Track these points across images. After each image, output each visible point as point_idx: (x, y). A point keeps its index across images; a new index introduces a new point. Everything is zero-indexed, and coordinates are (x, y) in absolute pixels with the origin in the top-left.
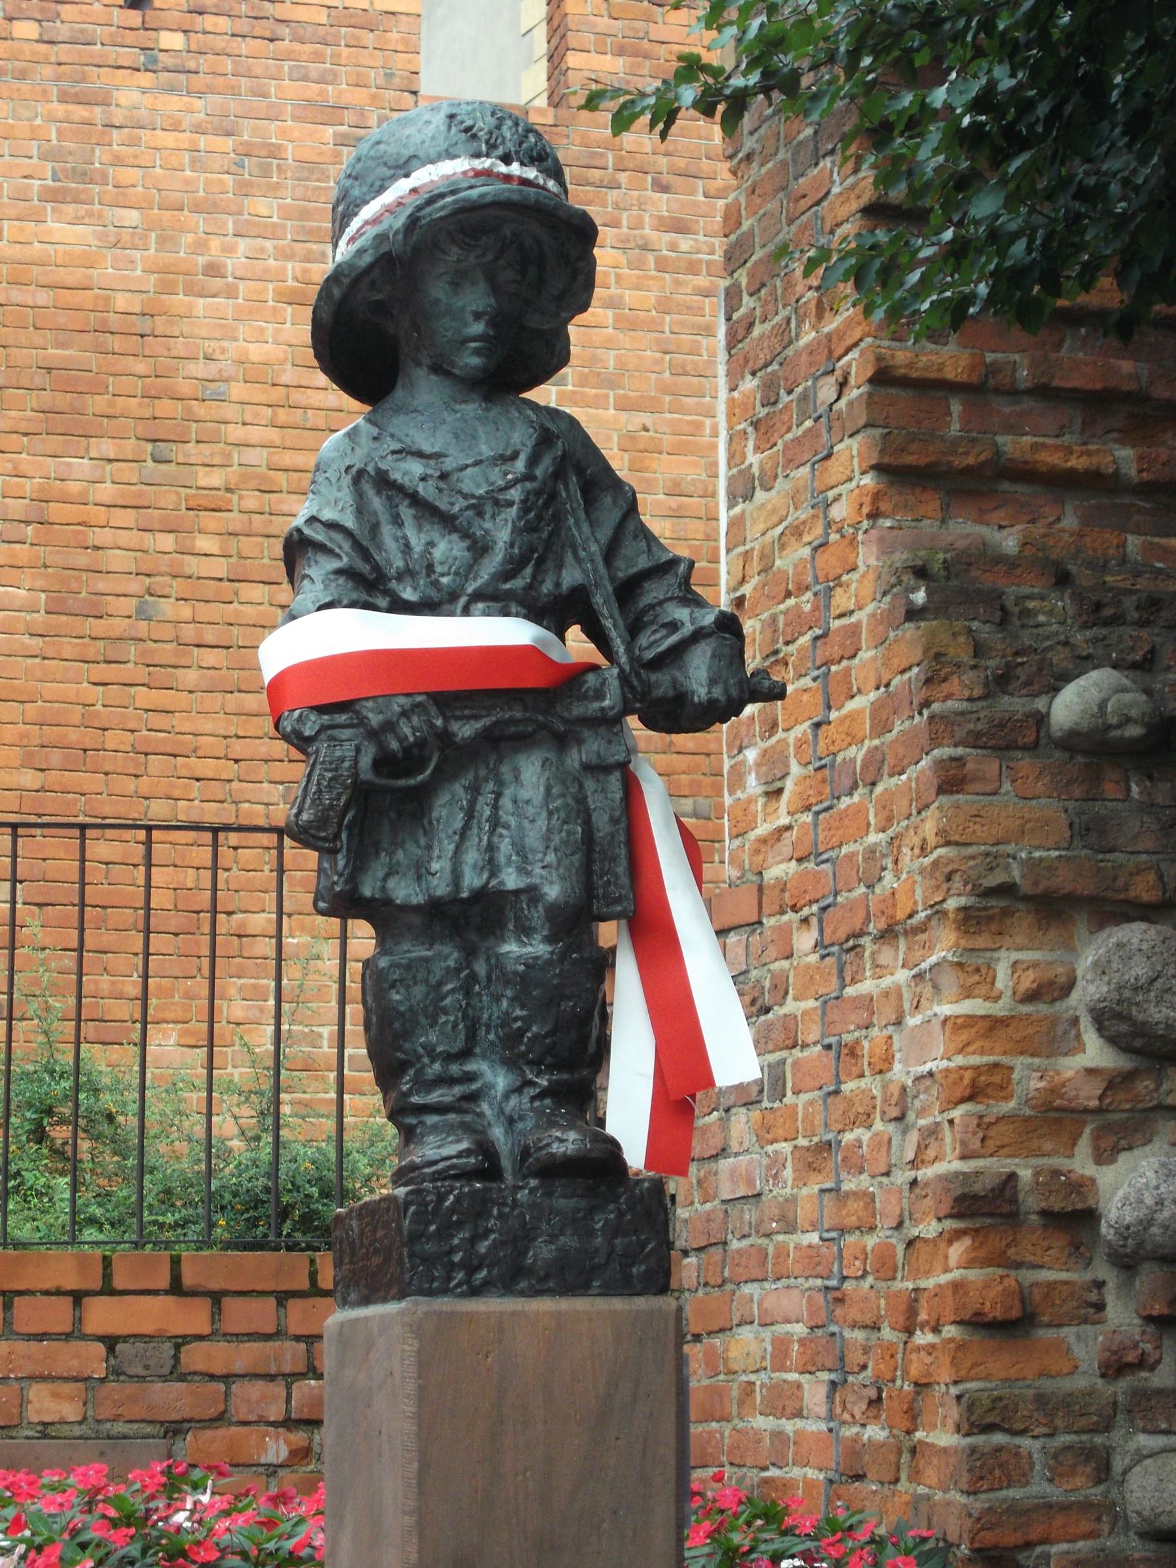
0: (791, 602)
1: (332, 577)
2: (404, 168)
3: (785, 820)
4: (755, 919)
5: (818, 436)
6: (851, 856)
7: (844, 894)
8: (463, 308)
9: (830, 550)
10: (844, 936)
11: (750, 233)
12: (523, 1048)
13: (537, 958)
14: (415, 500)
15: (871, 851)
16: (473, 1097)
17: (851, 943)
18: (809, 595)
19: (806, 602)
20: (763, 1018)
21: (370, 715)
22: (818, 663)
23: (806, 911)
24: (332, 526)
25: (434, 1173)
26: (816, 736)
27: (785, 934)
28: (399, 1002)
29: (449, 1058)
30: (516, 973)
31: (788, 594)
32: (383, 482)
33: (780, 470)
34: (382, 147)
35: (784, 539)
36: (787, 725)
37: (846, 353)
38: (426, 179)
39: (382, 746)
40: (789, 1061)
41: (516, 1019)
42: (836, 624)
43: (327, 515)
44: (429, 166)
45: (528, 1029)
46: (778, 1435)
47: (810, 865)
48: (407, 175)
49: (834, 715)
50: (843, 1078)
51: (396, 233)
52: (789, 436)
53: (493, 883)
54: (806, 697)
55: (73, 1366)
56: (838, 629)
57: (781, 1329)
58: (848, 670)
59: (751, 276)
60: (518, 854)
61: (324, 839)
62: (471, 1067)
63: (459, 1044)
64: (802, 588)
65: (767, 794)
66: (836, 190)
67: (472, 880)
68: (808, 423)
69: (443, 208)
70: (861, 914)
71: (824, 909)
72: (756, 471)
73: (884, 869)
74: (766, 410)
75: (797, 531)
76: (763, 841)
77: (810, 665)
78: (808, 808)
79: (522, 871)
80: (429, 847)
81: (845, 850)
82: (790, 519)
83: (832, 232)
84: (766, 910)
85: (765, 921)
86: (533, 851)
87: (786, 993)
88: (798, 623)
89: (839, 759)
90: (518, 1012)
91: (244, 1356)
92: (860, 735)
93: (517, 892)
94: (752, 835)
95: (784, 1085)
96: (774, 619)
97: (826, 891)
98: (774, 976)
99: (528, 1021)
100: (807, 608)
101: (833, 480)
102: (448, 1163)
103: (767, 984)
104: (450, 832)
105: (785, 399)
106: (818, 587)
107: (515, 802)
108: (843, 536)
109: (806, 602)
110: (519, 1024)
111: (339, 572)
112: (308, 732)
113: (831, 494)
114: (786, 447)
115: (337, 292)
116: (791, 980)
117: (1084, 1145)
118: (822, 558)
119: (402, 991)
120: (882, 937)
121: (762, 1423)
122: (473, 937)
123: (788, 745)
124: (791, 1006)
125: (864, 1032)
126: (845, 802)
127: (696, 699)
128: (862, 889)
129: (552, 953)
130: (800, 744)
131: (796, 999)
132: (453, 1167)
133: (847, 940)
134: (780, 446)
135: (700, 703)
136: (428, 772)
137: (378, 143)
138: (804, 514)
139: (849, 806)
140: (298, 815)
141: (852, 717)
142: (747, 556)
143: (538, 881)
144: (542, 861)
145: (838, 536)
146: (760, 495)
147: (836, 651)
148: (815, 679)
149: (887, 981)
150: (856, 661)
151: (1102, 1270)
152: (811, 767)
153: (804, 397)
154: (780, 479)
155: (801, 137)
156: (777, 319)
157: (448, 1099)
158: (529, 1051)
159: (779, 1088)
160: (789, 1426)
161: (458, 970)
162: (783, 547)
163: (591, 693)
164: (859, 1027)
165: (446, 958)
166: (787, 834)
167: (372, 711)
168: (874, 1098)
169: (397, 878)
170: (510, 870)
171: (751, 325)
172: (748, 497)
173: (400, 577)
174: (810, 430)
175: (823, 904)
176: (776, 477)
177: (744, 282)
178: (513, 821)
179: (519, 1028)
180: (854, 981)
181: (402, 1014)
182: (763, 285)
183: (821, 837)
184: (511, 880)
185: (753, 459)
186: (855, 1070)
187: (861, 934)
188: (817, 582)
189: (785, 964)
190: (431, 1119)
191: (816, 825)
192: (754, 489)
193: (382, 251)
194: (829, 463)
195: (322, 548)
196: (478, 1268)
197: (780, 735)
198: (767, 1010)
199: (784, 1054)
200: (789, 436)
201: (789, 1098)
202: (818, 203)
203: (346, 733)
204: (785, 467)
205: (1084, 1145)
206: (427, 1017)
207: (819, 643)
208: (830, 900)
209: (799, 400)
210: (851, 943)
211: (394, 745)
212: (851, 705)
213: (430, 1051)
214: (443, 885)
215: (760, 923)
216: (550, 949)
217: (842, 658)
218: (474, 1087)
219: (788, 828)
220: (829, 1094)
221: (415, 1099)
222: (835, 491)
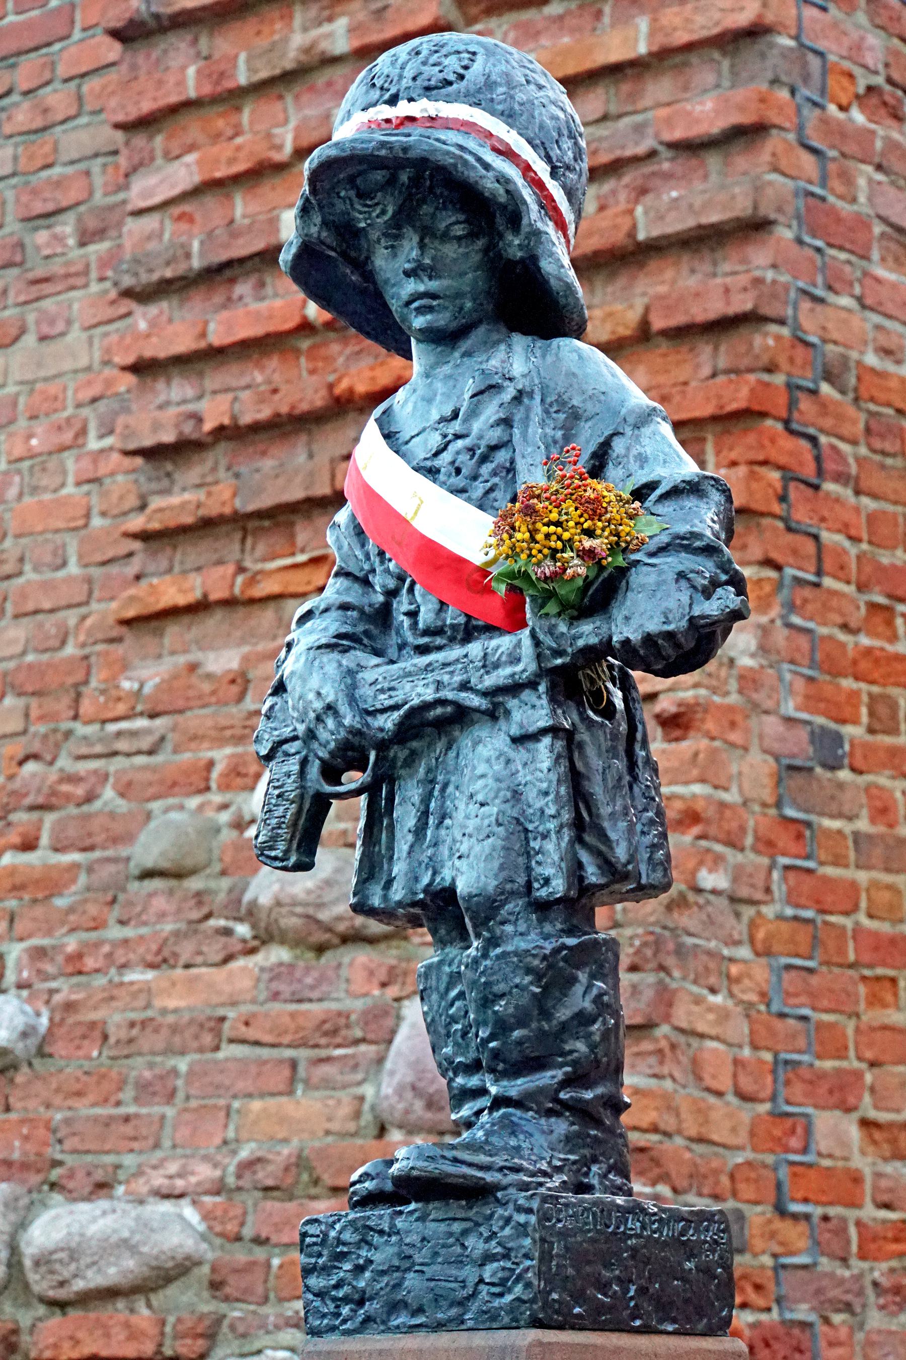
61: (275, 858)
196: (361, 1303)
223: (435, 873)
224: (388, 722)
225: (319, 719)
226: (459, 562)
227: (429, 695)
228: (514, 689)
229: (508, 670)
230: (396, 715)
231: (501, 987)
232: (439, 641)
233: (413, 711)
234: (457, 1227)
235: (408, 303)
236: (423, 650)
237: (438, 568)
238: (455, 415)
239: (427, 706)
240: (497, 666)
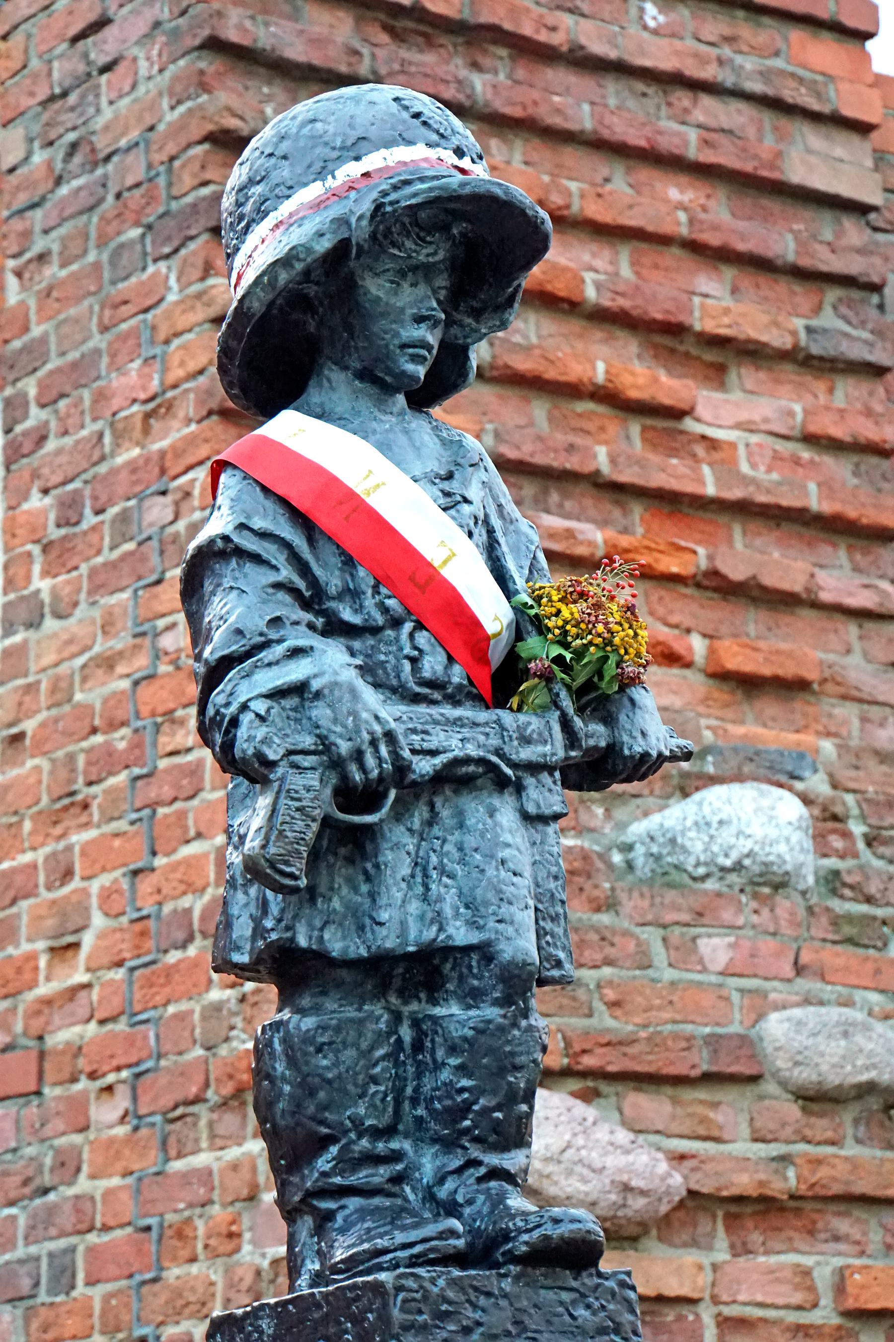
0: (98, 739)
1: (271, 591)
2: (355, 149)
3: (81, 977)
4: (33, 1087)
5: (144, 559)
6: (181, 1017)
7: (173, 1058)
8: (402, 310)
9: (157, 683)
10: (171, 1104)
11: (43, 340)
12: (467, 1123)
13: (489, 1022)
15: (217, 1007)
16: (398, 1179)
17: (179, 1111)
18: (125, 731)
19: (121, 740)
20: (38, 1201)
21: (339, 741)
22: (138, 804)
23: (111, 1078)
24: (264, 535)
25: (412, 1256)
26: (133, 885)
27: (79, 1105)
28: (327, 1068)
29: (378, 1133)
30: (465, 1039)
31: (94, 731)
33: (83, 596)
34: (319, 125)
35: (87, 671)
36: (88, 873)
37: (186, 472)
38: (381, 164)
39: (345, 777)
40: (81, 1249)
41: (462, 1090)
42: (163, 764)
43: (258, 523)
44: (383, 151)
45: (476, 1102)
47: (121, 1026)
48: (357, 158)
49: (160, 861)
50: (166, 1264)
51: (360, 218)
52: (100, 560)
53: (442, 937)
54: (117, 843)
56: (167, 771)
58: (182, 815)
59: (42, 386)
60: (467, 907)
62: (395, 1145)
63: (386, 1120)
64: (113, 725)
65: (52, 949)
66: (172, 297)
67: (419, 934)
68: (130, 546)
69: (415, 195)
70: (201, 1079)
71: (138, 1076)
72: (46, 596)
73: (232, 1028)
74: (63, 531)
75: (108, 663)
76: (48, 1002)
77: (126, 806)
78: (119, 964)
79: (473, 924)
80: (373, 896)
81: (171, 1009)
82: (97, 649)
83: (167, 342)
84: (49, 1076)
85: (46, 1091)
86: (487, 904)
87: (78, 1170)
88: (105, 763)
89: (167, 909)
90: (465, 1082)
92: (199, 883)
93: (468, 949)
94: (30, 996)
95: (74, 1276)
96: (71, 758)
97: (144, 1054)
98: (58, 1151)
99: (477, 1092)
100: (122, 745)
101: (162, 609)
102: (427, 1246)
103: (48, 1161)
104: (399, 877)
105: (90, 520)
106: (140, 723)
107: (461, 849)
108: (178, 668)
109: (121, 740)
110: (466, 1095)
111: (278, 586)
112: (272, 756)
113: (161, 623)
114: (93, 572)
115: (283, 277)
116: (85, 1156)
118: (146, 692)
119: (331, 1055)
120: (224, 1104)
122: (394, 1000)
123: (88, 895)
124: (83, 1185)
125: (198, 1211)
126: (174, 957)
127: (626, 752)
128: (199, 1052)
129: (504, 1016)
130: (106, 895)
131: (93, 1177)
132: (432, 1250)
133: (176, 1107)
134: (84, 569)
135: (632, 757)
136: (385, 810)
137: (314, 121)
138: (121, 642)
139: (180, 961)
140: (264, 847)
141: (189, 863)
143: (493, 937)
144: (494, 914)
145: (170, 668)
146: (50, 624)
147: (167, 792)
148: (132, 823)
149: (233, 1153)
150: (195, 802)
152: (124, 920)
153: (124, 517)
154: (83, 606)
155: (123, 238)
156: (84, 433)
157: (376, 1180)
158: (475, 1126)
159: (65, 1280)
161: (389, 1034)
162: (84, 679)
163: (535, 736)
164: (191, 1206)
165: (378, 1019)
166: (83, 994)
167: (341, 736)
168: (212, 1284)
169: (332, 927)
170: (458, 923)
171: (42, 439)
172: (33, 624)
173: (340, 597)
174: (131, 553)
175: (137, 1070)
176: (76, 604)
177: (32, 392)
178: (458, 869)
179: (464, 1101)
180: (180, 1156)
181: (329, 1082)
182: (63, 396)
183: (137, 996)
184: (461, 934)
185: (42, 585)
186: (185, 1253)
187: (198, 1100)
188: (138, 717)
189: (77, 1139)
190: (353, 1203)
191: (131, 983)
192: (42, 616)
193: (340, 237)
194: (159, 588)
195: (257, 559)
197: (76, 883)
198: (46, 1191)
199: (74, 1240)
200: (100, 560)
201: (81, 1289)
202: (146, 310)
203: (307, 761)
204: (90, 593)
206: (356, 1085)
207: (140, 783)
208: (150, 1064)
209: (113, 521)
210: (179, 1111)
211: (358, 777)
212: (186, 851)
213: (358, 1123)
214: (393, 936)
215: (38, 1093)
216: (502, 1012)
217: (175, 799)
218: (399, 1167)
219: (87, 986)
220: (144, 1283)
221: (338, 1180)
222: (168, 620)
223: (441, 929)
225: (374, 743)
226: (476, 624)
227: (472, 751)
228: (534, 768)
229: (540, 749)
230: (438, 761)
231: (523, 1059)
232: (437, 696)
233: (457, 762)
234: (565, 1296)
235: (404, 346)
236: (416, 699)
237: (457, 624)
238: (450, 476)
239: (467, 760)
240: (526, 740)
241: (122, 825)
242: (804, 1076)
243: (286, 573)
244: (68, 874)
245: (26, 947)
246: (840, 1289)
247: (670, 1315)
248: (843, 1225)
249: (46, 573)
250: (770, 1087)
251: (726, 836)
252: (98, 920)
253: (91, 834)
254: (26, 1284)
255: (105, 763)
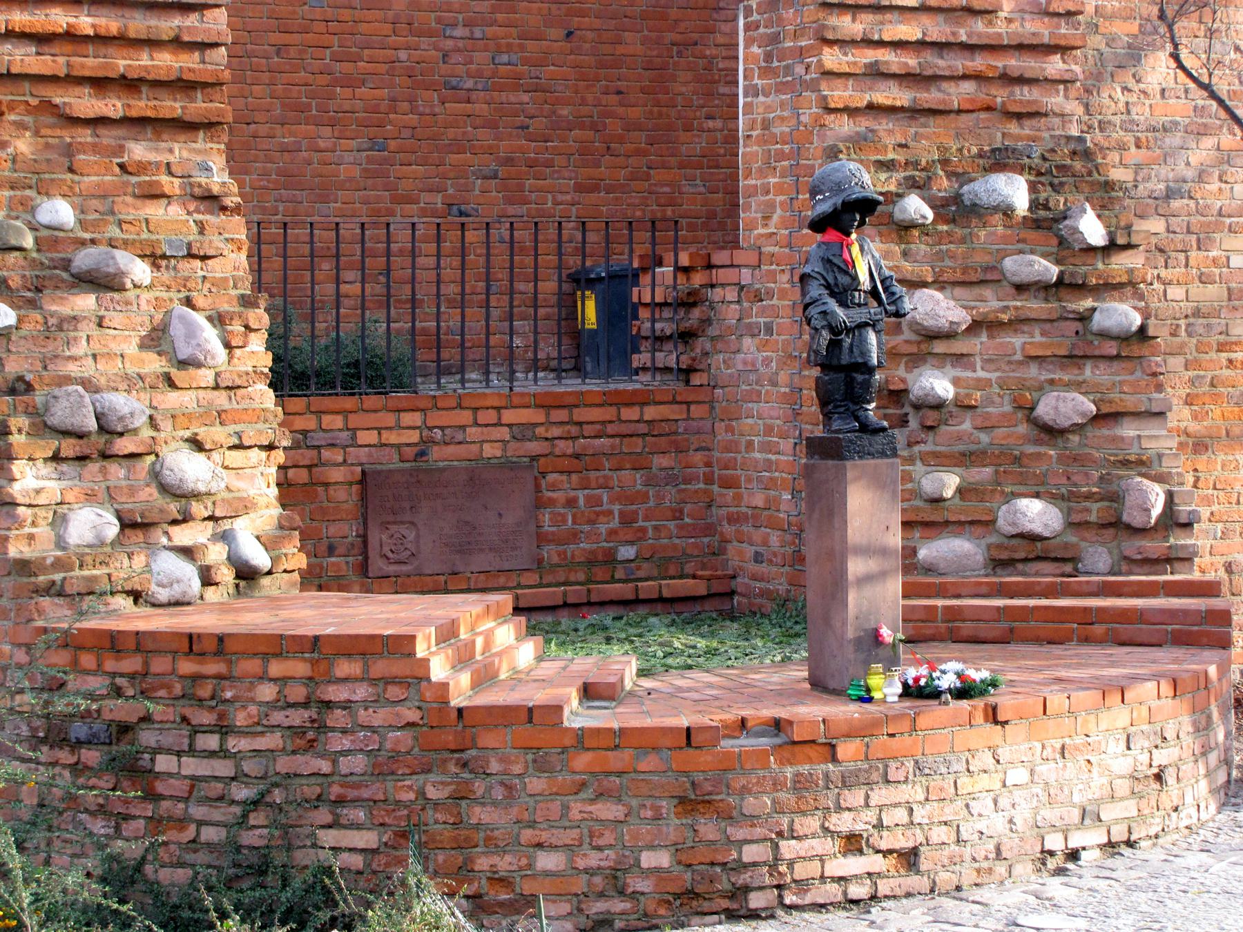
0: (778, 146)
14: (839, 267)
32: (829, 261)
46: (769, 460)
55: (498, 437)
57: (769, 421)
68: (790, 79)
91: (556, 432)
105: (775, 64)
117: (902, 366)
121: (757, 455)
124: (775, 301)
130: (782, 204)
142: (754, 121)
151: (907, 409)
160: (773, 457)
184: (860, 361)
197: (771, 196)
205: (902, 366)
224: (853, 325)
241: (787, 180)
242: (1016, 279)
243: (822, 282)
244: (768, 192)
245: (753, 215)
246: (1023, 349)
247: (965, 359)
248: (1026, 328)
249: (759, 77)
250: (1005, 283)
251: (995, 196)
252: (779, 211)
253: (776, 180)
254: (756, 331)
255: (781, 156)
